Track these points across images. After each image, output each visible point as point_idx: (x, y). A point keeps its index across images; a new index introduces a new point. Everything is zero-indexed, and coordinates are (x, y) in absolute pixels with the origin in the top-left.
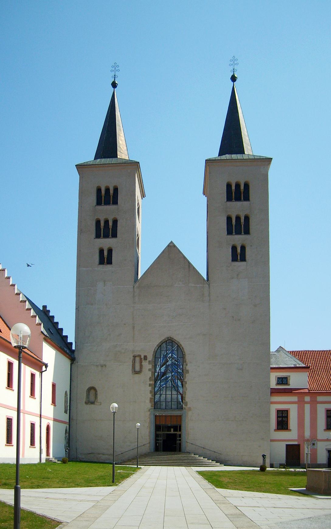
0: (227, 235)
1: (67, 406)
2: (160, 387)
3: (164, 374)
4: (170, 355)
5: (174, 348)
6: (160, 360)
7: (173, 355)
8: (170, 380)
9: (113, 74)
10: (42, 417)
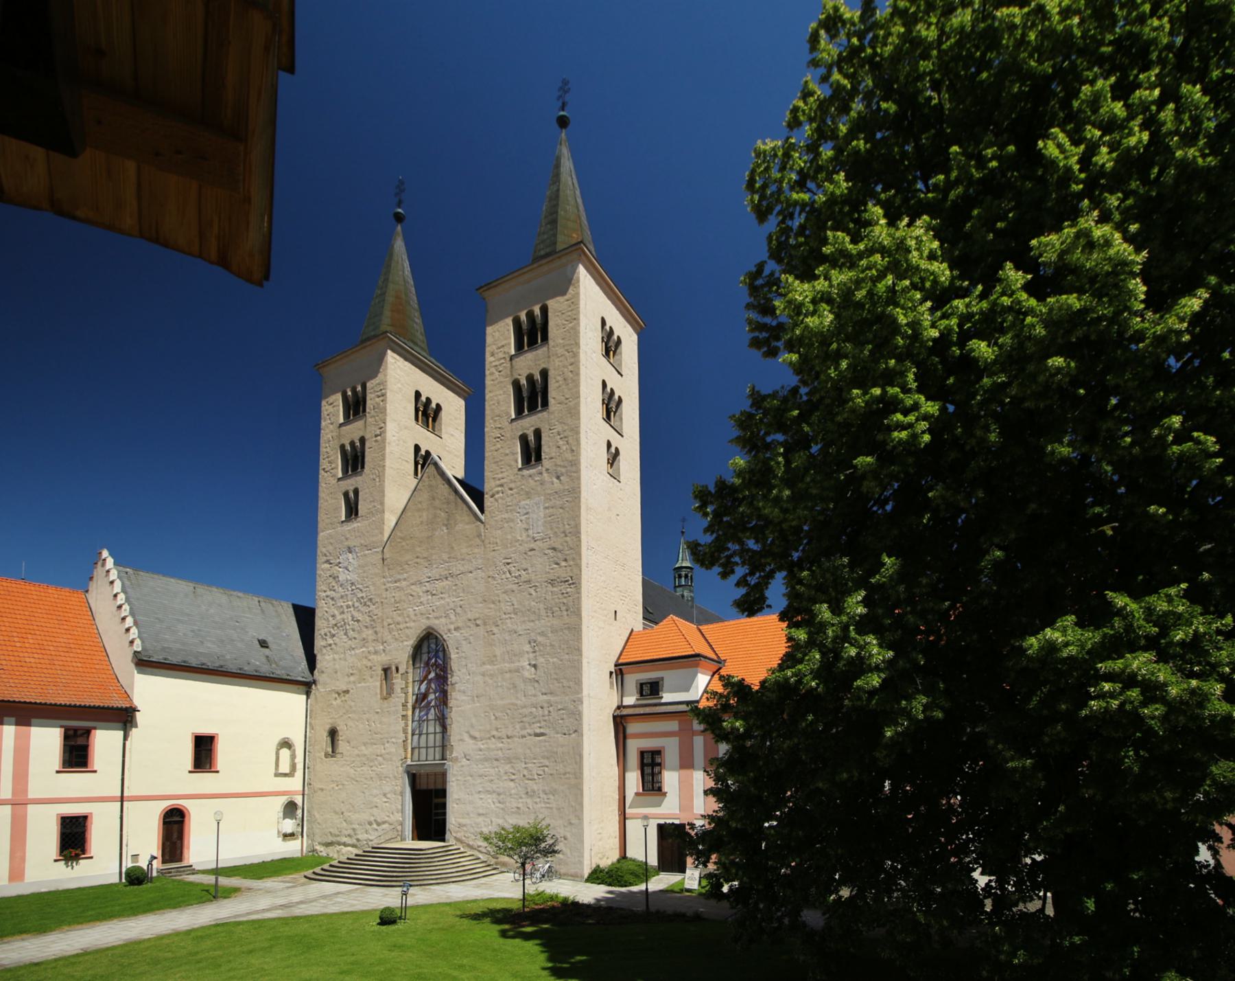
2: (419, 721)
3: (425, 696)
4: (433, 660)
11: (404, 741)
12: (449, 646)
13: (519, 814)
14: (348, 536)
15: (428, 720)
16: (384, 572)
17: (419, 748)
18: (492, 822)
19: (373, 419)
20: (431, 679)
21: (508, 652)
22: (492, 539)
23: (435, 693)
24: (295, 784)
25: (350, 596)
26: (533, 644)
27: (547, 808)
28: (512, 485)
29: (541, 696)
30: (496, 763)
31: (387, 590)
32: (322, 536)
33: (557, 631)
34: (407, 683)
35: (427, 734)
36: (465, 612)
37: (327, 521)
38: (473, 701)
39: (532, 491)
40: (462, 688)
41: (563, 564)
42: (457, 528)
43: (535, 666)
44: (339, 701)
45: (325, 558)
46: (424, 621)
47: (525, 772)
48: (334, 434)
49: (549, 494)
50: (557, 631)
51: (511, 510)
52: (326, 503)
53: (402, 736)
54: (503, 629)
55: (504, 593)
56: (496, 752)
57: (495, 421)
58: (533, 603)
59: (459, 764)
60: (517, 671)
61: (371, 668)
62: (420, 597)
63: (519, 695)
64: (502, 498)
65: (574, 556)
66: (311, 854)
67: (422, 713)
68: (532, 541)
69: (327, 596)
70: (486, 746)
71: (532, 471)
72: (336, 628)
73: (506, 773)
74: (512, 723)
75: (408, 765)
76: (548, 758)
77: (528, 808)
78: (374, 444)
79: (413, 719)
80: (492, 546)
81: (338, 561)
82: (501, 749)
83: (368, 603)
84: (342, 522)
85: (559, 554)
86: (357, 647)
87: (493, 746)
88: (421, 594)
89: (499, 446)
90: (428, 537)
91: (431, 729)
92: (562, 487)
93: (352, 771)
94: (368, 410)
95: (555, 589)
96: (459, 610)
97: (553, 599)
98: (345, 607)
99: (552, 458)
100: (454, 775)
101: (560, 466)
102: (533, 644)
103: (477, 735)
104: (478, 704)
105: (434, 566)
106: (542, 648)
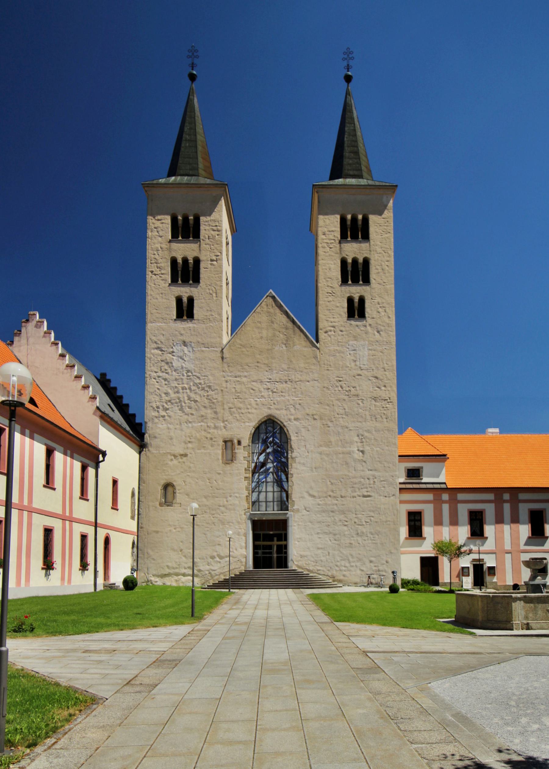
0: (341, 285)
1: (135, 510)
2: (258, 482)
3: (263, 464)
4: (271, 439)
5: (276, 430)
6: (257, 446)
7: (275, 439)
8: (271, 472)
10: (98, 526)
11: (247, 496)
12: (289, 430)
13: (351, 547)
14: (183, 332)
15: (267, 482)
16: (223, 367)
18: (329, 553)
19: (208, 246)
20: (269, 453)
21: (341, 440)
22: (326, 362)
23: (273, 463)
25: (185, 381)
26: (360, 437)
30: (332, 514)
31: (227, 382)
32: (150, 327)
33: (379, 431)
35: (266, 492)
36: (304, 408)
38: (312, 470)
39: (358, 336)
40: (302, 461)
41: (383, 388)
42: (295, 348)
43: (363, 452)
45: (155, 346)
46: (266, 410)
47: (356, 520)
49: (372, 341)
50: (379, 431)
51: (342, 345)
53: (246, 493)
54: (337, 425)
55: (337, 400)
56: (331, 506)
58: (360, 410)
59: (300, 514)
60: (349, 453)
61: (211, 439)
62: (261, 392)
64: (333, 335)
67: (261, 477)
68: (359, 369)
69: (159, 377)
70: (323, 502)
72: (169, 403)
73: (340, 521)
74: (345, 488)
75: (251, 514)
76: (373, 511)
77: (359, 543)
78: (210, 266)
80: (326, 366)
81: (172, 350)
82: (336, 505)
83: (206, 389)
84: (175, 319)
85: (380, 382)
86: (194, 422)
87: (329, 502)
88: (262, 390)
89: (330, 299)
90: (268, 350)
91: (270, 489)
92: (381, 339)
94: (201, 237)
96: (298, 406)
97: (376, 410)
98: (180, 388)
99: (373, 318)
100: (296, 522)
101: (380, 325)
102: (360, 437)
103: (315, 494)
104: (316, 473)
105: (275, 372)
106: (368, 441)
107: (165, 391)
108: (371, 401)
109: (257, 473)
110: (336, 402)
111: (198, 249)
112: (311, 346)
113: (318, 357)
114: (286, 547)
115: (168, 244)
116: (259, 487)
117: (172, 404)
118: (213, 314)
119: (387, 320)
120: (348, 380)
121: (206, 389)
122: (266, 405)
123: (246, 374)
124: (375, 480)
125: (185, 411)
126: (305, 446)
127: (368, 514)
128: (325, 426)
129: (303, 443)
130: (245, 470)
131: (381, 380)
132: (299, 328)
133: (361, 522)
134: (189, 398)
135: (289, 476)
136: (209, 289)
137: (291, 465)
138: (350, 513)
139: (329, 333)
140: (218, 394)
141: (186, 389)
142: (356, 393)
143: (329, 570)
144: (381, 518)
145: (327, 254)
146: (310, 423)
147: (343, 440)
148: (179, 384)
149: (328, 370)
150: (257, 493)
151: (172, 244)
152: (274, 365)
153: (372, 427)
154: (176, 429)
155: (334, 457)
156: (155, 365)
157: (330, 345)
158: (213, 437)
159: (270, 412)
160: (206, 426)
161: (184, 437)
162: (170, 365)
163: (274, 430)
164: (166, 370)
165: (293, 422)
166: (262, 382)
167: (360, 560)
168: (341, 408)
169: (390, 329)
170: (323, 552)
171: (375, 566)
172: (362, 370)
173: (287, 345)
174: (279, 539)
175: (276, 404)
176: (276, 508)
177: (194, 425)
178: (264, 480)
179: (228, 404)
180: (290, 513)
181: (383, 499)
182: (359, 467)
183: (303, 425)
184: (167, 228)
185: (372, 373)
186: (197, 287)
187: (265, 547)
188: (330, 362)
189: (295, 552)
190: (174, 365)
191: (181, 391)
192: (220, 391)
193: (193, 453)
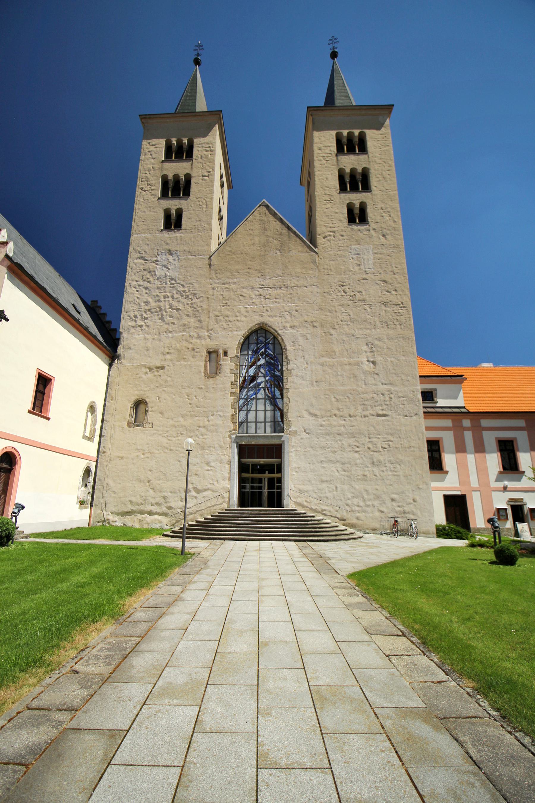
2: (246, 399)
3: (253, 378)
4: (263, 350)
6: (247, 358)
8: (263, 388)
9: (196, 52)
11: (232, 415)
13: (366, 480)
14: (168, 242)
15: (257, 399)
16: (210, 274)
17: (247, 422)
18: (336, 488)
19: (200, 164)
20: (260, 366)
23: (265, 376)
24: (91, 449)
25: (168, 289)
27: (394, 475)
28: (342, 233)
29: (381, 385)
30: (338, 437)
31: (213, 289)
32: (135, 238)
34: (236, 365)
35: (256, 410)
36: (301, 315)
37: (144, 227)
38: (312, 384)
40: (300, 374)
41: (394, 292)
43: (374, 363)
44: (150, 375)
45: (139, 255)
46: (257, 317)
47: (370, 446)
48: (156, 166)
49: (377, 245)
51: (343, 250)
52: (143, 214)
53: (231, 411)
56: (337, 428)
57: (325, 190)
58: (368, 316)
60: (357, 364)
61: (193, 349)
62: (251, 298)
63: (360, 384)
64: (332, 239)
65: (403, 288)
66: (101, 524)
67: (250, 393)
68: (364, 273)
69: (139, 286)
70: (327, 422)
71: (360, 227)
73: (350, 446)
74: (354, 405)
75: (237, 436)
76: (391, 434)
78: (201, 181)
79: (239, 397)
80: (326, 271)
81: (156, 259)
82: (344, 426)
84: (162, 230)
85: (390, 285)
86: (175, 331)
87: (335, 423)
88: (253, 296)
89: (328, 206)
90: (260, 256)
91: (261, 407)
92: (387, 242)
93: (165, 440)
94: (194, 157)
95: (387, 309)
96: (294, 313)
97: (387, 315)
98: (162, 297)
99: (377, 223)
100: (293, 446)
103: (318, 413)
105: (268, 277)
106: (379, 350)
107: (145, 300)
108: (380, 306)
109: (245, 388)
110: (338, 308)
111: (190, 167)
112: (309, 251)
113: (317, 262)
114: (280, 480)
115: (160, 165)
116: (247, 404)
117: (152, 313)
118: (202, 223)
119: (393, 225)
120: (352, 285)
121: (190, 297)
122: (257, 312)
123: (235, 280)
124: (392, 396)
125: (166, 320)
126: (304, 356)
127: (385, 438)
128: (327, 333)
129: (301, 353)
130: (231, 384)
131: (390, 284)
132: (295, 233)
133: (376, 448)
134: (171, 307)
135: (284, 391)
136: (199, 201)
137: (287, 379)
138: (362, 436)
139: (329, 238)
140: (203, 301)
141: (168, 297)
142: (362, 297)
143: (337, 511)
144: (402, 443)
145: (324, 166)
146: (309, 331)
147: (349, 350)
148: (160, 293)
149: (328, 274)
150: (246, 412)
151: (164, 164)
152: (267, 271)
153: (383, 334)
154: (153, 339)
155: (339, 370)
156: (137, 274)
157: (330, 249)
158: (195, 347)
159: (261, 319)
160: (188, 336)
161: (162, 348)
162: (153, 273)
163: (266, 340)
164: (148, 279)
165: (288, 330)
166: (253, 288)
167: (378, 497)
168: (345, 314)
169: (397, 232)
170: (329, 486)
171: (399, 507)
172: (367, 274)
173: (281, 251)
174: (272, 471)
175: (269, 310)
176: (268, 429)
177: (174, 334)
178: (254, 396)
179: (215, 312)
180: (285, 437)
181: (403, 419)
182: (371, 380)
183: (301, 334)
184: (160, 151)
185: (379, 276)
186: (186, 200)
187: (253, 480)
188: (330, 266)
189: (293, 486)
190: (157, 273)
191: (163, 299)
192: (206, 299)
193: (171, 365)
